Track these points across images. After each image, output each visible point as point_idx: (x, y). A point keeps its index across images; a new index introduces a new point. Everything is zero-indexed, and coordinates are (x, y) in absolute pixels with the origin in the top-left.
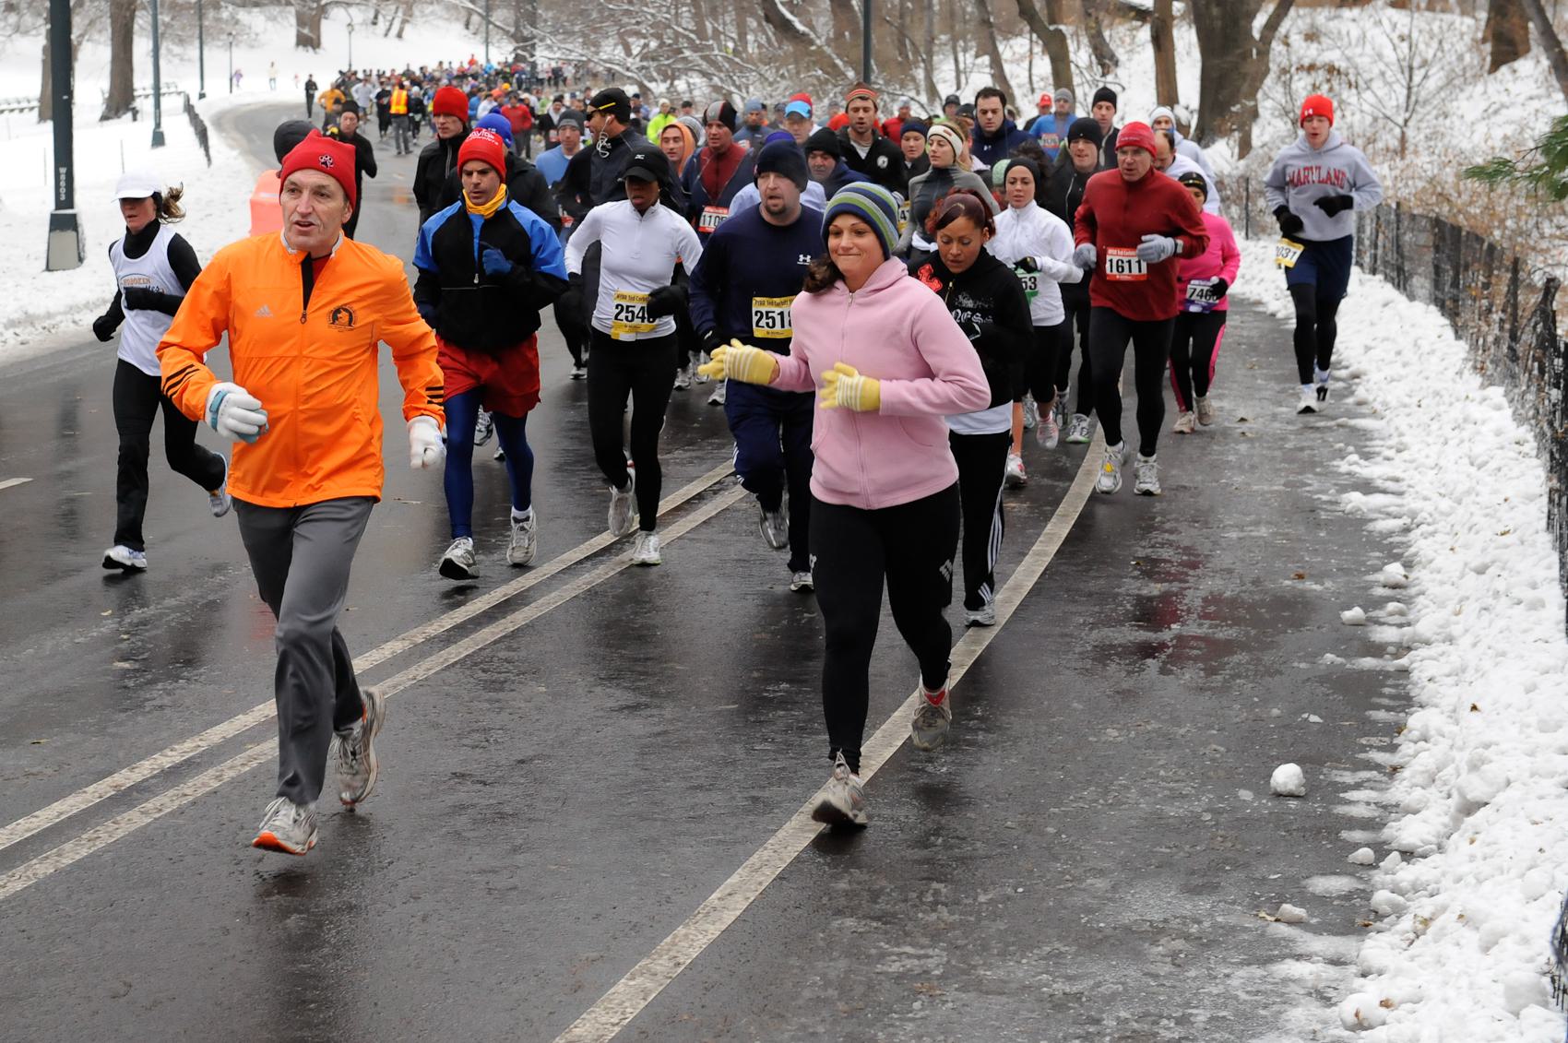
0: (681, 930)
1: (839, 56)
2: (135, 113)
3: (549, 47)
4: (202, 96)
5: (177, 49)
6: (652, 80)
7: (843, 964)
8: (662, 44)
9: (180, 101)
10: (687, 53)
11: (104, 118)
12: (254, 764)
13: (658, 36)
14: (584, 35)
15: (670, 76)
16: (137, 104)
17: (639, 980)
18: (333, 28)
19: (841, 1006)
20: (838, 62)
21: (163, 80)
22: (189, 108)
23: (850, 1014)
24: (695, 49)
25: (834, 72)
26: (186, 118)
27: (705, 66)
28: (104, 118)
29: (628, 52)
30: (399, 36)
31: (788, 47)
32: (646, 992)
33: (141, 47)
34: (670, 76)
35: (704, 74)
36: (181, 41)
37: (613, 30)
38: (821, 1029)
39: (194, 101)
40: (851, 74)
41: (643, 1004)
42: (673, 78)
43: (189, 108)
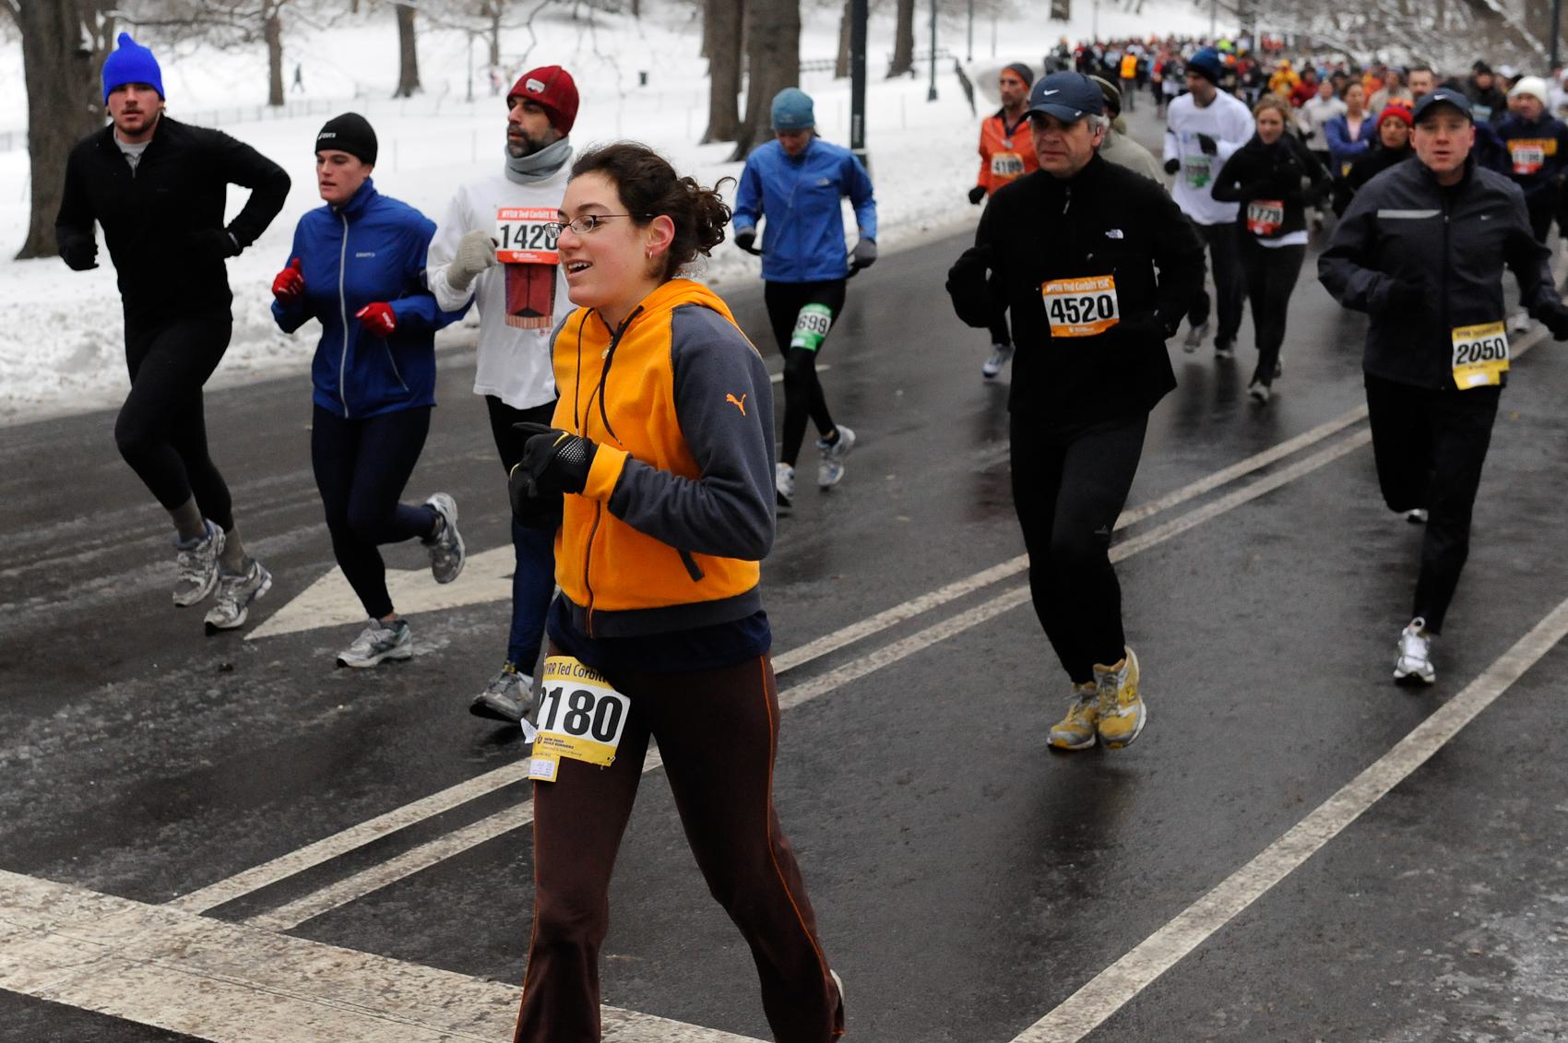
0: (1380, 764)
1: (1530, 31)
2: (913, 72)
3: (1268, 23)
4: (969, 59)
5: (950, 20)
6: (1356, 48)
7: (1525, 802)
8: (1368, 21)
9: (950, 65)
10: (1391, 28)
11: (889, 76)
12: (1013, 605)
13: (1366, 13)
14: (1299, 12)
15: (1373, 46)
16: (917, 65)
17: (1343, 802)
18: (1079, 7)
19: (1523, 837)
20: (1529, 37)
21: (940, 45)
22: (959, 70)
23: (1535, 843)
24: (1398, 24)
25: (1524, 46)
26: (955, 79)
27: (1405, 39)
28: (889, 76)
29: (1337, 25)
30: (1138, 11)
31: (1482, 24)
32: (1350, 812)
33: (921, 19)
34: (1373, 46)
35: (1407, 47)
36: (953, 14)
37: (1325, 8)
38: (1505, 855)
39: (963, 63)
40: (1539, 47)
41: (1345, 823)
42: (1377, 48)
43: (959, 70)
